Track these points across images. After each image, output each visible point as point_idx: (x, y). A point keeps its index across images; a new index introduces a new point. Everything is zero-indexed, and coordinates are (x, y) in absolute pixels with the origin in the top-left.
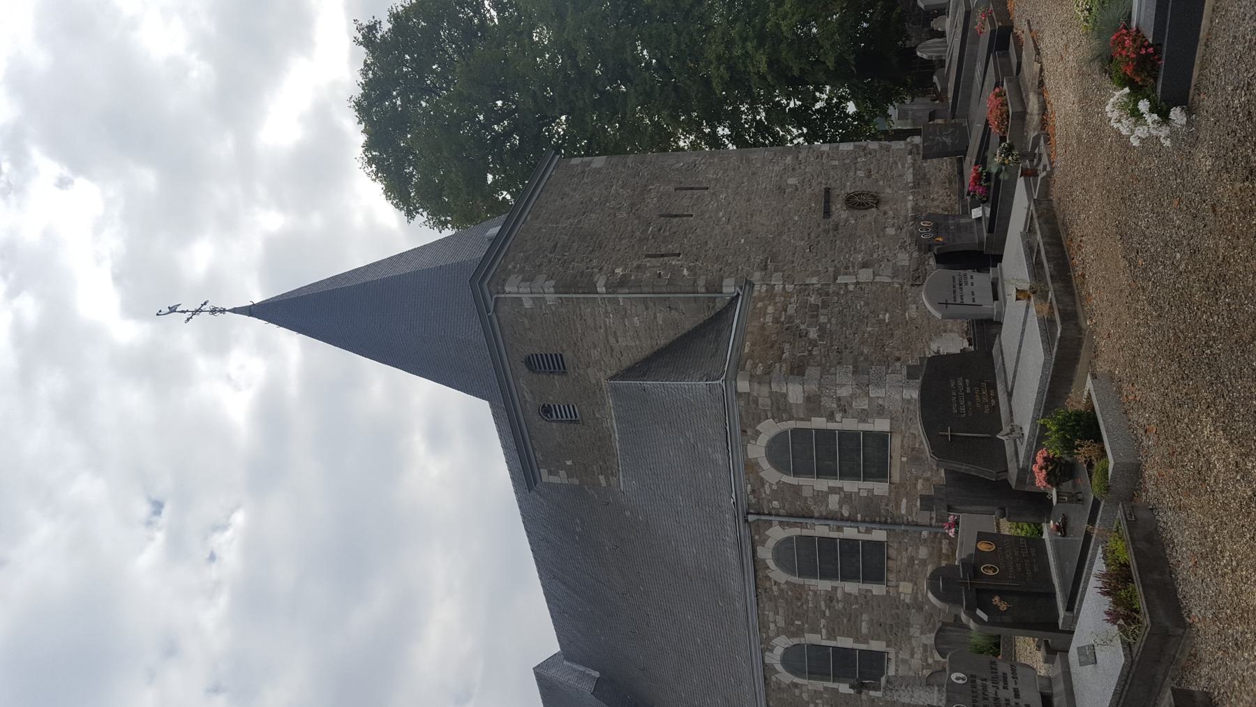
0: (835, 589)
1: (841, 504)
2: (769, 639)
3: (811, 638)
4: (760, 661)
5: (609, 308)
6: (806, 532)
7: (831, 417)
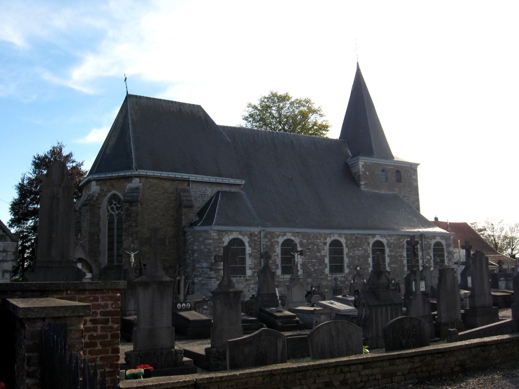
0: (404, 257)
1: (428, 259)
2: (385, 237)
3: (387, 250)
4: (377, 233)
5: (414, 199)
6: (419, 250)
7: (447, 257)
